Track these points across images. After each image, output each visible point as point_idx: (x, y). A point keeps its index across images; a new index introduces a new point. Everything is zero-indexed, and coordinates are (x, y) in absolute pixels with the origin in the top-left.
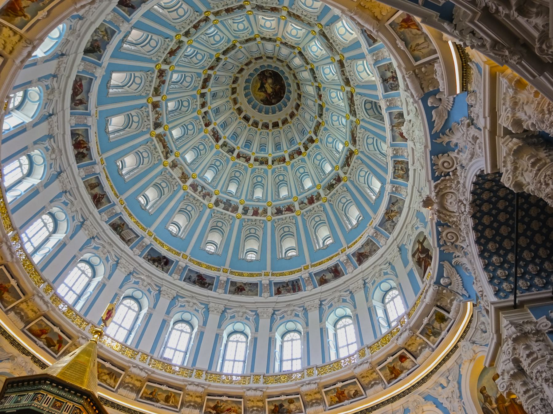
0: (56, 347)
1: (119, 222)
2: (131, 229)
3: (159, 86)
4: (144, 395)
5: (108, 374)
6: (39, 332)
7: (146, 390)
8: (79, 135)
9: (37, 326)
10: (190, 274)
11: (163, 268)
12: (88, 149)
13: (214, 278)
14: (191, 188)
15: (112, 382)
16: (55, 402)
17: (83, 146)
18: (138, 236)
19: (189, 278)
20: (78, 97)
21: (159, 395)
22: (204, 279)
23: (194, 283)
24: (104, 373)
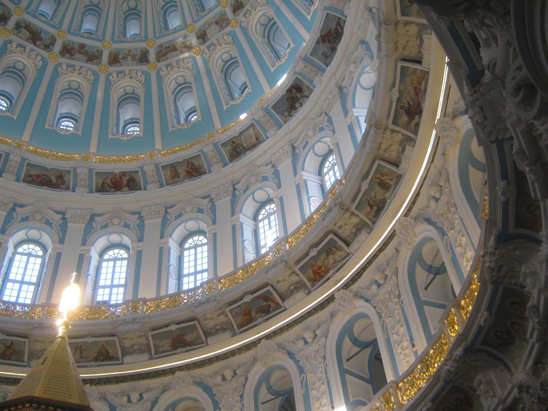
0: (273, 305)
1: (229, 148)
2: (241, 133)
3: (87, 53)
5: (328, 255)
6: (246, 318)
8: (103, 183)
10: (320, 54)
11: (306, 96)
12: (124, 174)
13: (328, 15)
14: (237, 12)
15: (339, 254)
17: (119, 180)
18: (252, 125)
19: (326, 57)
20: (54, 180)
21: (375, 196)
22: (329, 32)
23: (334, 50)
24: (325, 259)
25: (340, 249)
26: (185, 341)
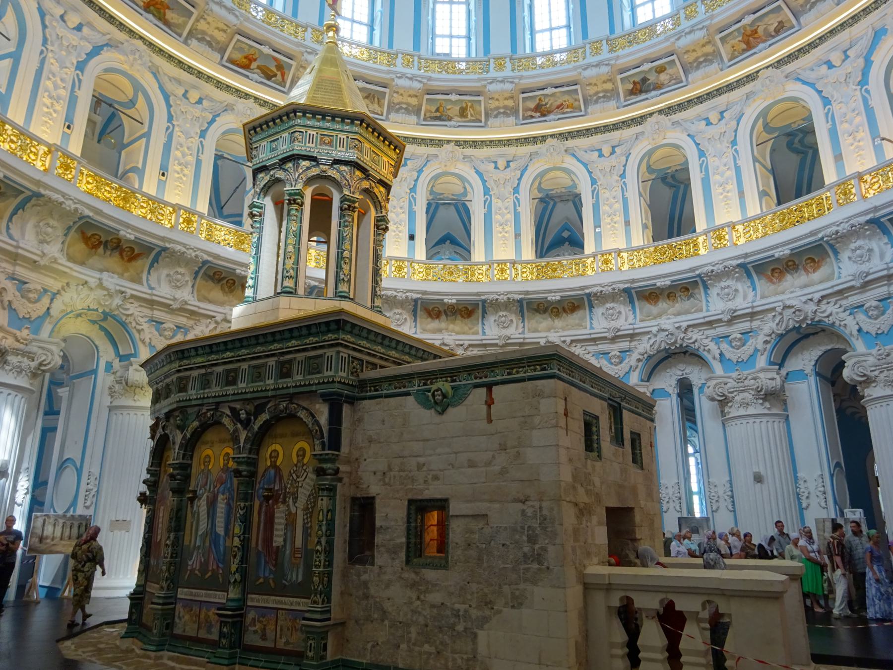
4: (428, 115)
6: (245, 60)
7: (429, 107)
9: (237, 52)
16: (321, 139)
21: (449, 109)
25: (380, 105)
26: (165, 14)
